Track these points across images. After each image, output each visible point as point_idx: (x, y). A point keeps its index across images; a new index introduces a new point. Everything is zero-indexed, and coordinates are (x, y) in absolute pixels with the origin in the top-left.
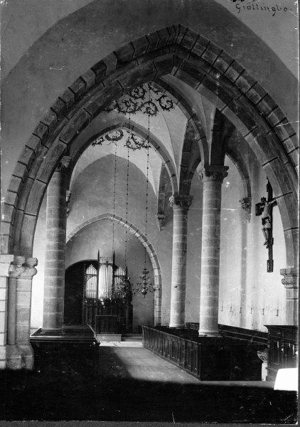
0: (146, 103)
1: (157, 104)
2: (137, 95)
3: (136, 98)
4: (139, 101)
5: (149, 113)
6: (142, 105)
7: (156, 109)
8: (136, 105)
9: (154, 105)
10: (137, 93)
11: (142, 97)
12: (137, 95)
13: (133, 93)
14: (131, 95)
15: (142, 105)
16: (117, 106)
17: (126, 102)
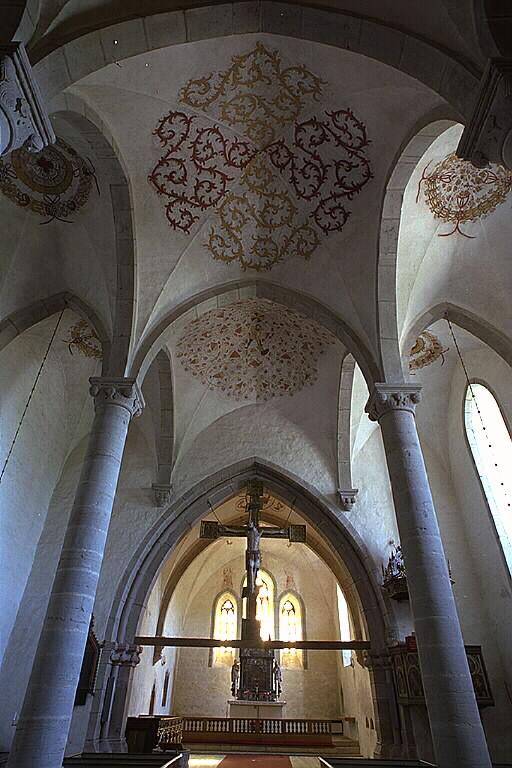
0: (215, 97)
1: (189, 111)
2: (238, 102)
3: (237, 97)
4: (231, 95)
5: (198, 83)
6: (221, 91)
7: (187, 100)
8: (236, 81)
9: (195, 105)
10: (237, 108)
11: (224, 106)
12: (238, 102)
13: (247, 102)
14: (249, 96)
15: (221, 91)
16: (282, 77)
17: (260, 77)
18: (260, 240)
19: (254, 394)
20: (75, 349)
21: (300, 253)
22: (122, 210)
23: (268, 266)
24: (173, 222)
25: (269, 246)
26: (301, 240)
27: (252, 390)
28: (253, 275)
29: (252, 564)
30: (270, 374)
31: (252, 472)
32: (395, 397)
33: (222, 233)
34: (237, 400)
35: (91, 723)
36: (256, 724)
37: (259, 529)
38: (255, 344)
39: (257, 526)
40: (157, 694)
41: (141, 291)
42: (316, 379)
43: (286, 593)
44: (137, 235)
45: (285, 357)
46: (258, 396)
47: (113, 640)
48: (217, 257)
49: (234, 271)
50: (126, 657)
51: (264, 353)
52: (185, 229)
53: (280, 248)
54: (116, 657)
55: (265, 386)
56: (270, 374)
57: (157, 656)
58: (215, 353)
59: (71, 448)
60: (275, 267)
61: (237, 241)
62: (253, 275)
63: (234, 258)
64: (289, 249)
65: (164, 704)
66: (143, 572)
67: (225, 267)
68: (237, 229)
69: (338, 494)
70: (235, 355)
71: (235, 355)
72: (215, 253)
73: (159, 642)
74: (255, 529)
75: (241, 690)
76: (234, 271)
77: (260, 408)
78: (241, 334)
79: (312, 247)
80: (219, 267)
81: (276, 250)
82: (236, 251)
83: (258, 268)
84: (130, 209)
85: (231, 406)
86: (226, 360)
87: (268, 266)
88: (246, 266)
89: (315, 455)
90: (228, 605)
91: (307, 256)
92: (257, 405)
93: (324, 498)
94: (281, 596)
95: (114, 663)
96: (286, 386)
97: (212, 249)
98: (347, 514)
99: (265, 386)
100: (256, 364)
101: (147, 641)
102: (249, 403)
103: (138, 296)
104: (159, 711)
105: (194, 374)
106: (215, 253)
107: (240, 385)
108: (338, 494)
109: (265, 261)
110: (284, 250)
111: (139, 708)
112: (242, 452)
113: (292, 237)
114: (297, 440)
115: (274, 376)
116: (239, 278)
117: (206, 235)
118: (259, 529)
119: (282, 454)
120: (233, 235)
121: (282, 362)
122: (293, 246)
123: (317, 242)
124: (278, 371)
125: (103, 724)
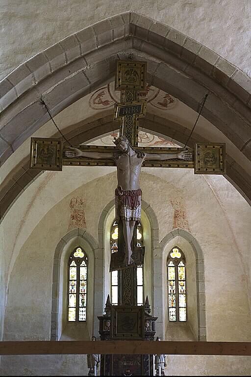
29: (128, 213)
31: (124, 45)
37: (140, 152)
39: (134, 145)
43: (172, 235)
74: (132, 152)
90: (79, 254)
94: (165, 240)
119: (184, 6)
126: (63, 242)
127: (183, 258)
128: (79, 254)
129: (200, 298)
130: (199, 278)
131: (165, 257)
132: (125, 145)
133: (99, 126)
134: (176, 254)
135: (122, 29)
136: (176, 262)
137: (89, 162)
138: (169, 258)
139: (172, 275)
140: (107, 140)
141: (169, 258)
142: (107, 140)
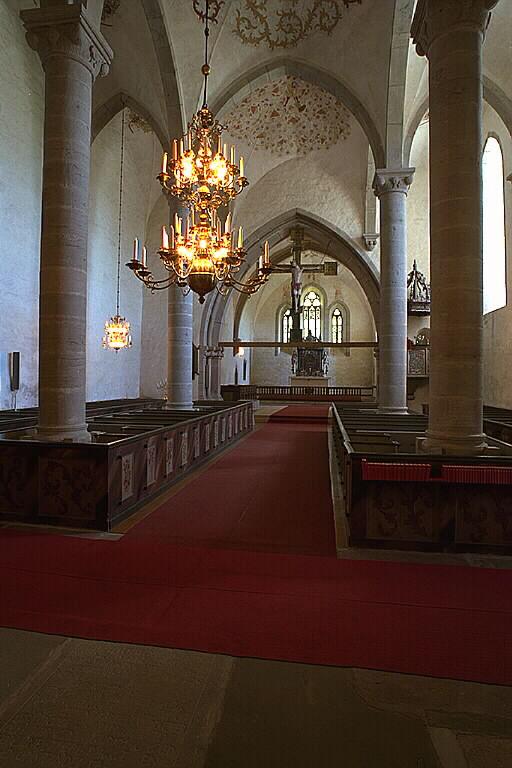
18: (285, 15)
19: (295, 148)
20: (134, 127)
21: (323, 28)
22: (155, 18)
23: (294, 42)
24: (200, 14)
25: (293, 21)
26: (324, 14)
27: (292, 145)
28: (280, 53)
29: (296, 293)
30: (308, 129)
32: (391, 180)
33: (247, 14)
34: (280, 156)
35: (200, 389)
36: (309, 390)
37: (301, 267)
38: (292, 102)
39: (298, 264)
40: (239, 373)
41: (185, 93)
42: (349, 134)
43: (334, 303)
44: (172, 39)
45: (321, 112)
46: (298, 151)
47: (205, 345)
48: (246, 40)
49: (260, 52)
50: (214, 354)
51: (301, 109)
52: (213, 19)
53: (303, 23)
54: (208, 354)
55: (304, 141)
56: (308, 129)
57: (236, 351)
58: (256, 116)
59: (150, 211)
60: (300, 44)
61: (263, 20)
62: (280, 53)
63: (260, 39)
64: (313, 24)
65: (244, 379)
66: (218, 301)
67: (254, 50)
68: (262, 6)
69: (363, 238)
70: (274, 114)
71: (274, 114)
72: (243, 37)
73: (236, 344)
75: (298, 370)
76: (260, 52)
77: (300, 162)
78: (279, 93)
79: (333, 22)
80: (249, 50)
81: (301, 25)
82: (263, 31)
83: (284, 44)
84: (161, 17)
85: (276, 162)
86: (267, 120)
87: (294, 42)
88: (272, 44)
89: (347, 204)
91: (330, 30)
92: (298, 159)
93: (352, 241)
94: (330, 306)
95: (208, 358)
96: (323, 140)
97: (239, 33)
98: (369, 254)
99: (304, 141)
100: (294, 120)
101: (228, 345)
102: (290, 157)
103: (183, 101)
104: (241, 382)
105: (239, 138)
106: (243, 37)
107: (281, 142)
108: (363, 238)
109: (290, 36)
110: (308, 24)
111: (228, 380)
112: (285, 205)
113: (314, 10)
114: (332, 190)
115: (312, 131)
116: (268, 58)
117: (233, 20)
118: (301, 267)
120: (259, 14)
121: (318, 117)
122: (316, 20)
123: (338, 16)
124: (315, 126)
125: (207, 388)
126: (278, 310)
127: (341, 315)
128: (288, 313)
129: (348, 334)
130: (348, 324)
131: (331, 312)
132: (295, 264)
133: (285, 254)
134: (337, 313)
135: (294, 213)
136: (337, 316)
137: (280, 271)
138: (333, 315)
139: (334, 323)
140: (287, 262)
141: (333, 315)
142: (287, 262)
